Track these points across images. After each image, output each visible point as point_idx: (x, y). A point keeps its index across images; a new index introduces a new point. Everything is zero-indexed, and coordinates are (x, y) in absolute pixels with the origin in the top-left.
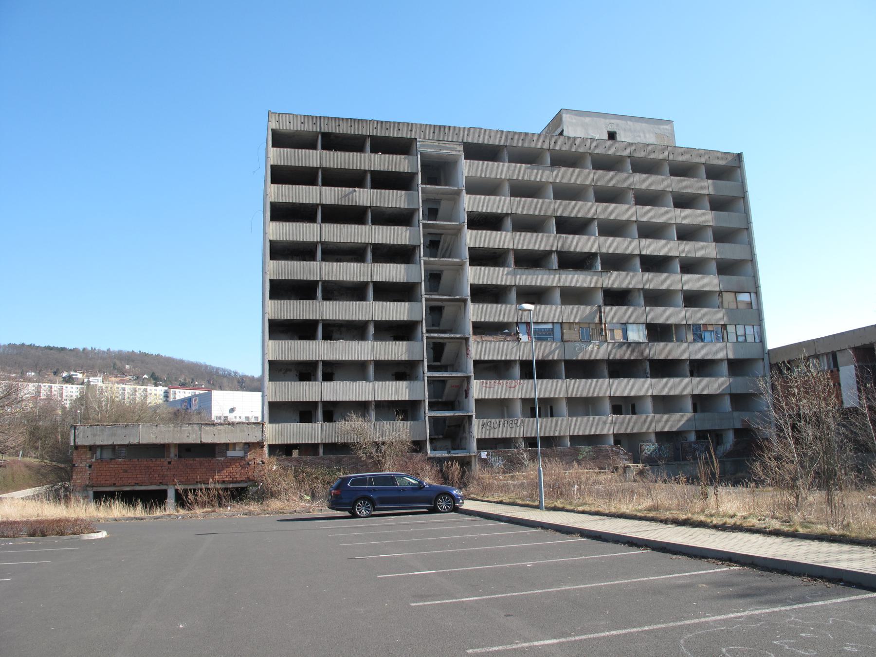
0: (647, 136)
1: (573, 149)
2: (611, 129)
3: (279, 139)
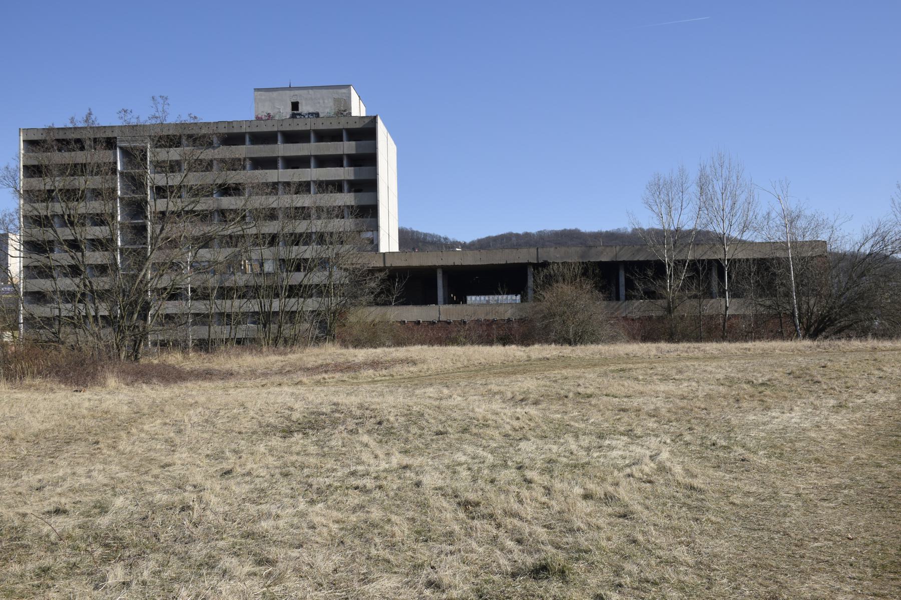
0: (326, 101)
1: (231, 131)
2: (294, 100)
3: (32, 144)
